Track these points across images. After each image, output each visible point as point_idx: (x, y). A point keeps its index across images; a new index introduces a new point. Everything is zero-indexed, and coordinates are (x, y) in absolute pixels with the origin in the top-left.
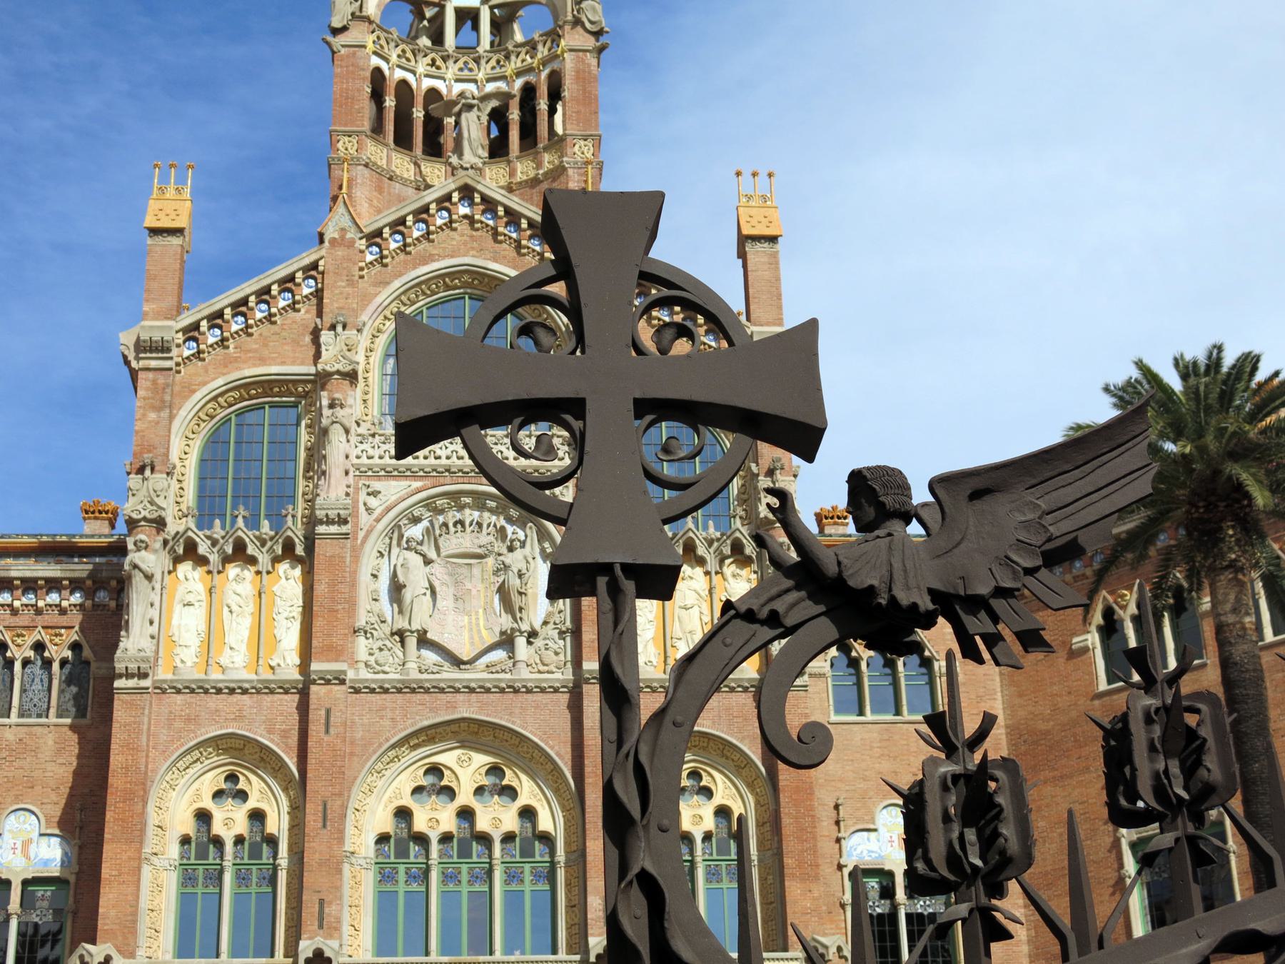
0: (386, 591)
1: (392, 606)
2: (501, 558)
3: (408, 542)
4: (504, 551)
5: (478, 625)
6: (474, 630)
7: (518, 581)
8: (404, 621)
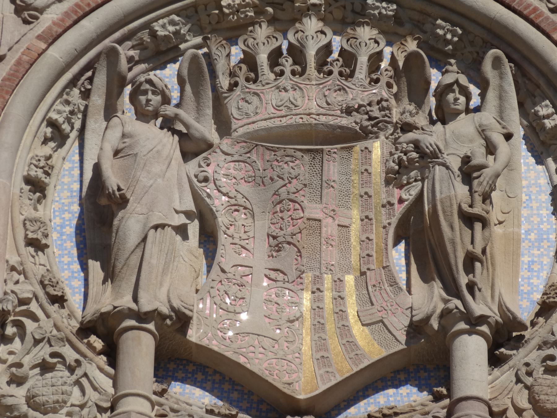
0: (70, 230)
1: (84, 268)
2: (411, 136)
3: (133, 98)
4: (421, 120)
5: (341, 314)
6: (330, 327)
7: (462, 190)
8: (117, 294)
